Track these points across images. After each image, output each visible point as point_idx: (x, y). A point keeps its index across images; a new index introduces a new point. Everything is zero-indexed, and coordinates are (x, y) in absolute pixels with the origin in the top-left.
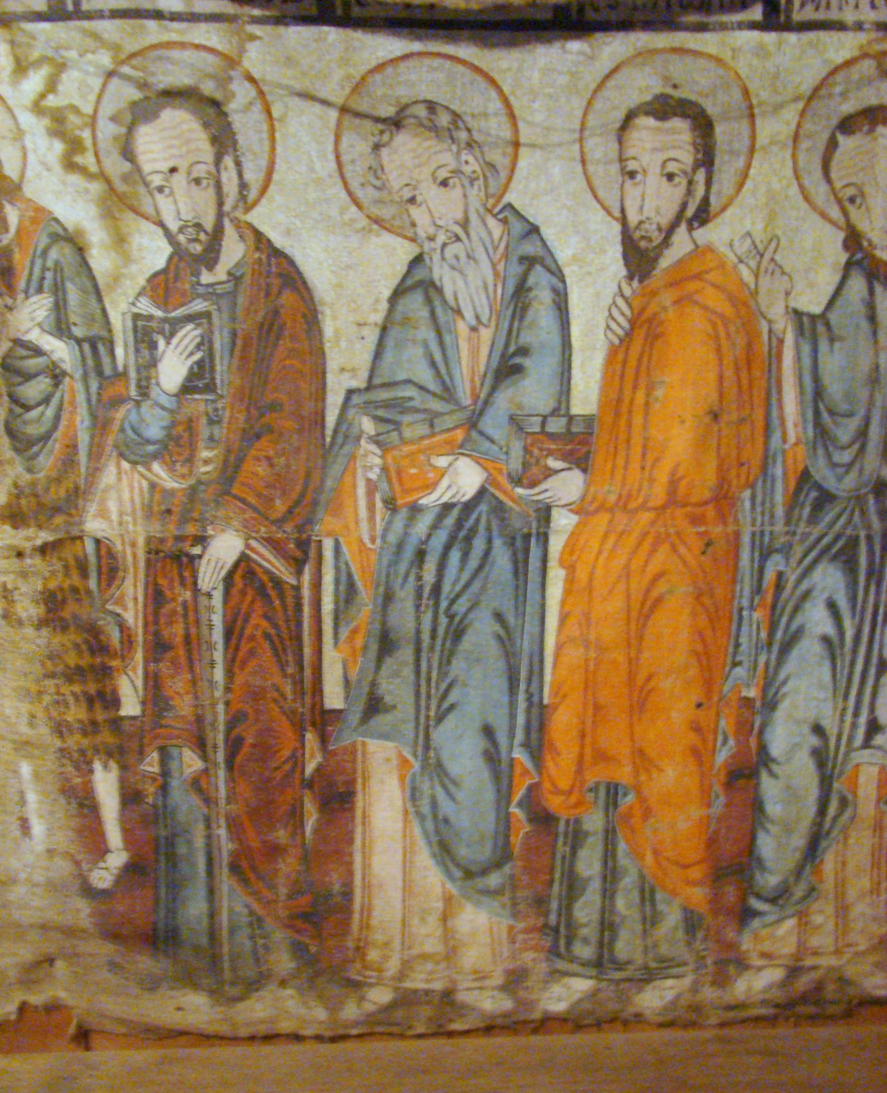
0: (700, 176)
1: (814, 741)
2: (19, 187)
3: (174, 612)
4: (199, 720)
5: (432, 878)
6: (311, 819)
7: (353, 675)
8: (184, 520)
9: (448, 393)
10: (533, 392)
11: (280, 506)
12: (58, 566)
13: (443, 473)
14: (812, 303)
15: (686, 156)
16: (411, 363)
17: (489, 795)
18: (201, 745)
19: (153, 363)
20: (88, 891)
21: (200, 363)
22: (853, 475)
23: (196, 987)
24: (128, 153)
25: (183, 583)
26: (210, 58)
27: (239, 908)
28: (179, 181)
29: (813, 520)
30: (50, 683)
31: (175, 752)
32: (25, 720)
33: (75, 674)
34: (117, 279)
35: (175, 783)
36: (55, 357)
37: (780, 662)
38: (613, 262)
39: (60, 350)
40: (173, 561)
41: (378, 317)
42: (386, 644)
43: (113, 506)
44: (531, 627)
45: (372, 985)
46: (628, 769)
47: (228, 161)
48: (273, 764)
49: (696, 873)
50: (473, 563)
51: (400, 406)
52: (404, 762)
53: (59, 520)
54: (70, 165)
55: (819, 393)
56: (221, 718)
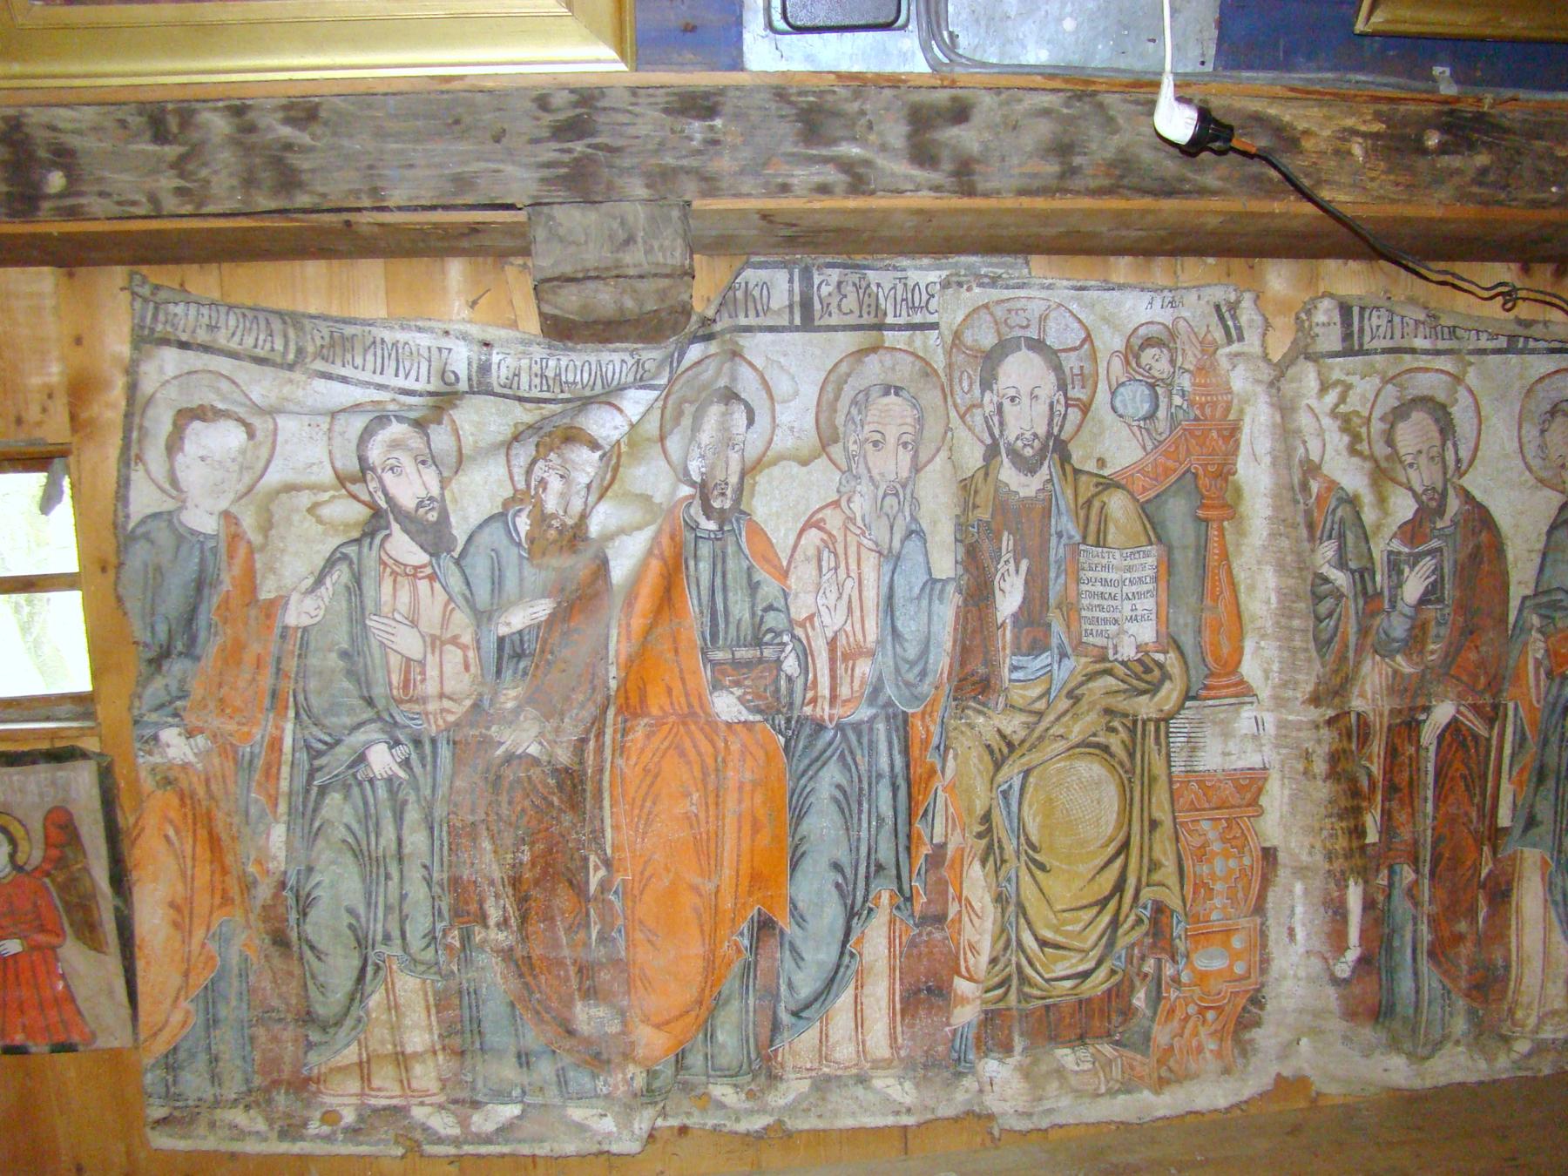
2: (1319, 467)
3: (1402, 764)
4: (1416, 842)
7: (1519, 804)
8: (1414, 697)
12: (1336, 734)
18: (1415, 861)
19: (1400, 585)
20: (1335, 981)
21: (1434, 584)
23: (1399, 1050)
24: (1390, 442)
25: (1410, 741)
26: (1444, 377)
27: (1435, 984)
28: (1423, 460)
31: (1397, 868)
34: (1378, 527)
35: (1396, 892)
36: (1337, 583)
39: (1340, 578)
40: (1408, 725)
41: (1540, 546)
43: (1368, 688)
45: (1517, 1039)
47: (1449, 444)
48: (1460, 872)
52: (1545, 862)
53: (1337, 700)
54: (1353, 451)
56: (1429, 840)
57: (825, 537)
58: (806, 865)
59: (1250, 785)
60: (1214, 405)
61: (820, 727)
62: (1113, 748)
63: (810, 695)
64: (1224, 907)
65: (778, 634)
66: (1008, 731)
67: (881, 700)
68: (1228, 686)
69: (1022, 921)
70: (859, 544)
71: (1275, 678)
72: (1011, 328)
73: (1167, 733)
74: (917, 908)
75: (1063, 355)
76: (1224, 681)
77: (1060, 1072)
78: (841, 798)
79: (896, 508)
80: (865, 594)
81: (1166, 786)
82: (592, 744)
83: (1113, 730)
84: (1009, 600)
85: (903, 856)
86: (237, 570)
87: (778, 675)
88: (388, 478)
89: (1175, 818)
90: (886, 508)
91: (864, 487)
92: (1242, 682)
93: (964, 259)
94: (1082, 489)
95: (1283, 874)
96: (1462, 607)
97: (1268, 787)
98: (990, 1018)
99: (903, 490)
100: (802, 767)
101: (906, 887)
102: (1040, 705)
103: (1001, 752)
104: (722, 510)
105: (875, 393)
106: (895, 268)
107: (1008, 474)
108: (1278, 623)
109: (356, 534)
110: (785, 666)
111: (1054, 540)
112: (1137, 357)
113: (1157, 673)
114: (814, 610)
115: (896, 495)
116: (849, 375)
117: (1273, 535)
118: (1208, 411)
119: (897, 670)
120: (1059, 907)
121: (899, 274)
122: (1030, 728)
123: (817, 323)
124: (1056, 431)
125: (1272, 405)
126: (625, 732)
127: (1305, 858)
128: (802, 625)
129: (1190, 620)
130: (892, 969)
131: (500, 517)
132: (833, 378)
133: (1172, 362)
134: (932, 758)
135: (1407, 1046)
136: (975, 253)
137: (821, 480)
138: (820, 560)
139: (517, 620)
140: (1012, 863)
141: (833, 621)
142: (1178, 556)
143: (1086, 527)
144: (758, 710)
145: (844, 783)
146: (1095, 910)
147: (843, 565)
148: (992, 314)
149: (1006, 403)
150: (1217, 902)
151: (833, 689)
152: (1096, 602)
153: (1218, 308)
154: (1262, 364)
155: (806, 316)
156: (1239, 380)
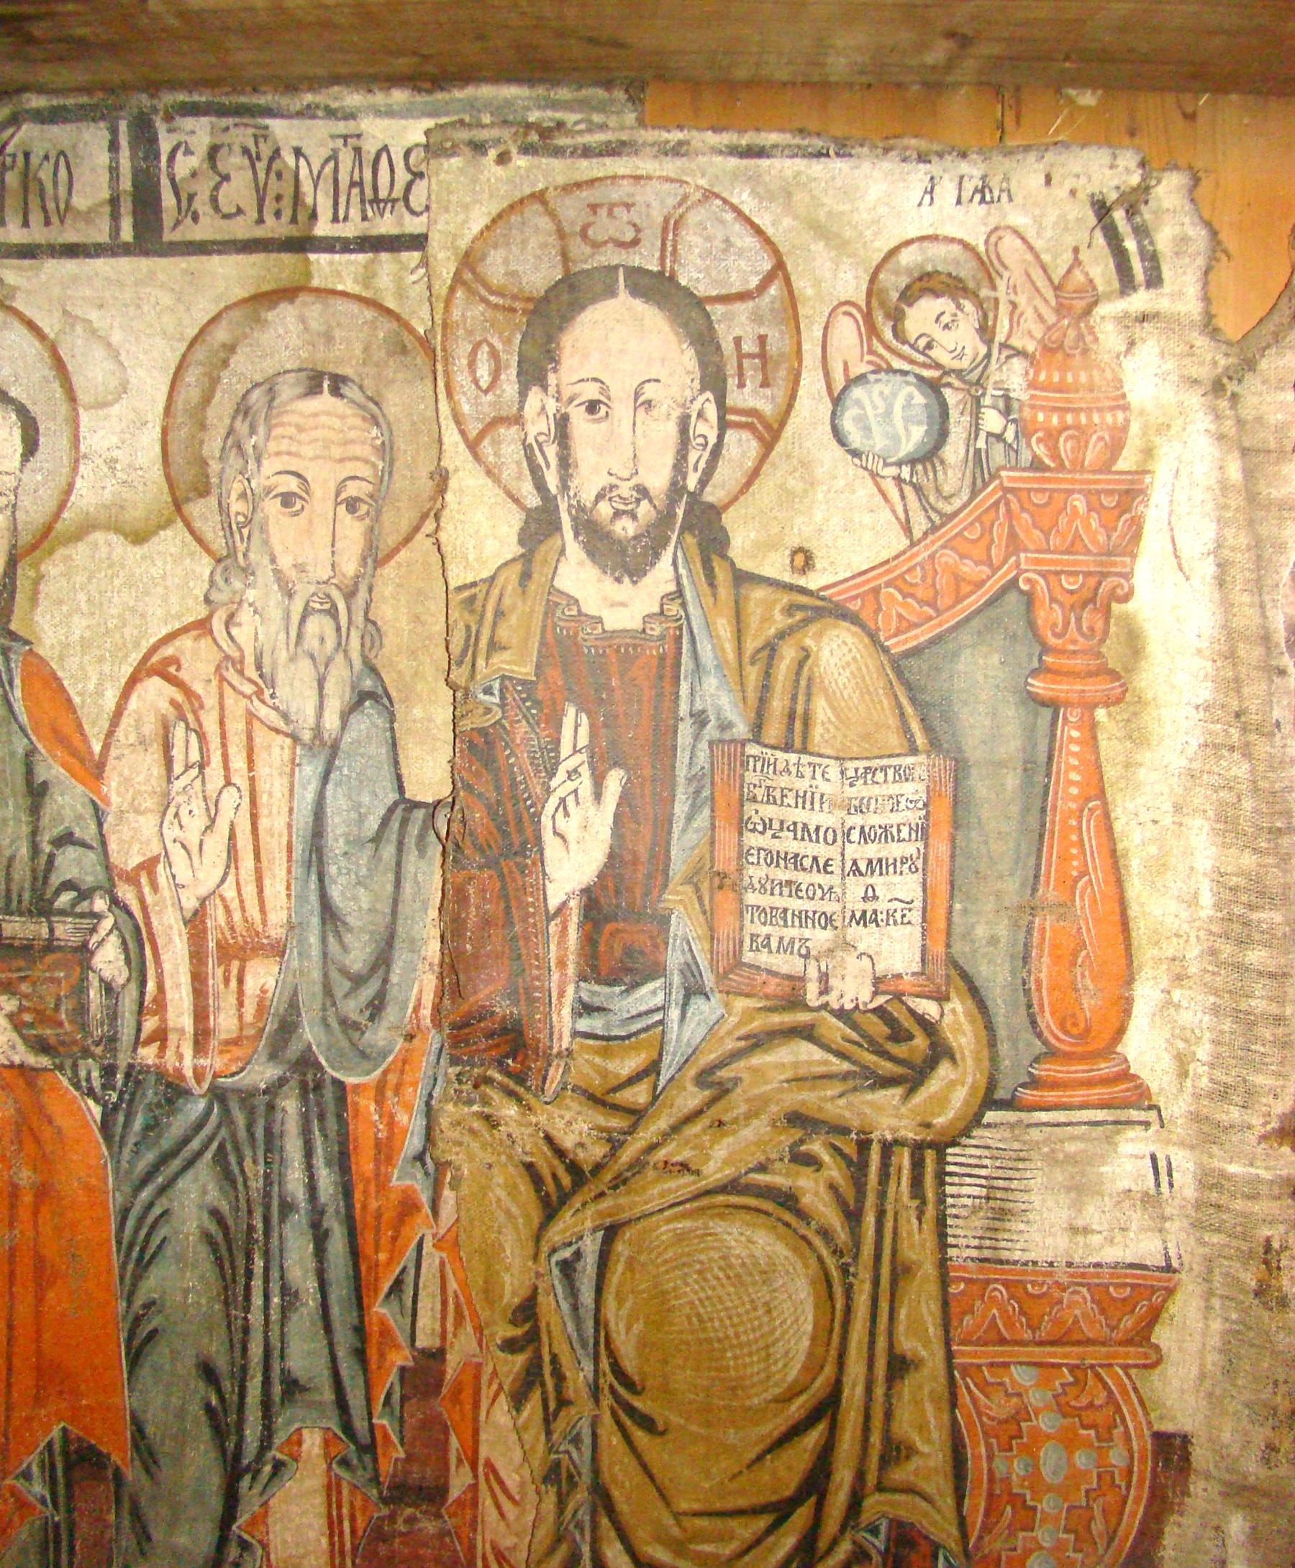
32: (1255, 1454)
57: (180, 698)
58: (159, 1354)
59: (1137, 1302)
60: (1081, 434)
61: (174, 1091)
62: (806, 1200)
63: (150, 1024)
64: (1059, 1547)
66: (568, 1142)
68: (1089, 1083)
69: (605, 1522)
70: (251, 717)
72: (596, 245)
73: (941, 1176)
74: (386, 1468)
75: (717, 311)
76: (1078, 1070)
78: (220, 1238)
79: (330, 643)
80: (264, 823)
81: (933, 1288)
83: (811, 1161)
84: (574, 853)
85: (348, 1368)
87: (84, 979)
89: (949, 1355)
90: (311, 642)
91: (262, 592)
92: (1125, 1075)
93: (486, 91)
94: (753, 620)
95: (1201, 1492)
97: (1174, 1307)
99: (349, 601)
100: (142, 1165)
101: (360, 1424)
102: (639, 1095)
103: (558, 1183)
105: (286, 390)
106: (331, 113)
107: (578, 576)
108: (1213, 952)
110: (99, 961)
111: (685, 732)
112: (897, 318)
113: (920, 1042)
114: (156, 849)
115: (333, 613)
116: (231, 348)
117: (1212, 747)
118: (1065, 447)
119: (328, 991)
120: (684, 1506)
121: (341, 127)
123: (168, 236)
124: (692, 482)
125: (1221, 437)
128: (132, 878)
129: (1002, 930)
132: (200, 354)
133: (986, 332)
136: (518, 81)
137: (169, 578)
138: (167, 747)
140: (581, 1412)
141: (197, 874)
142: (979, 785)
143: (763, 701)
144: (42, 1047)
145: (225, 1207)
146: (762, 1522)
147: (216, 758)
148: (552, 214)
149: (578, 417)
150: (1043, 1535)
151: (201, 1015)
152: (782, 875)
153: (1102, 209)
154: (1201, 342)
155: (146, 224)
156: (1150, 377)
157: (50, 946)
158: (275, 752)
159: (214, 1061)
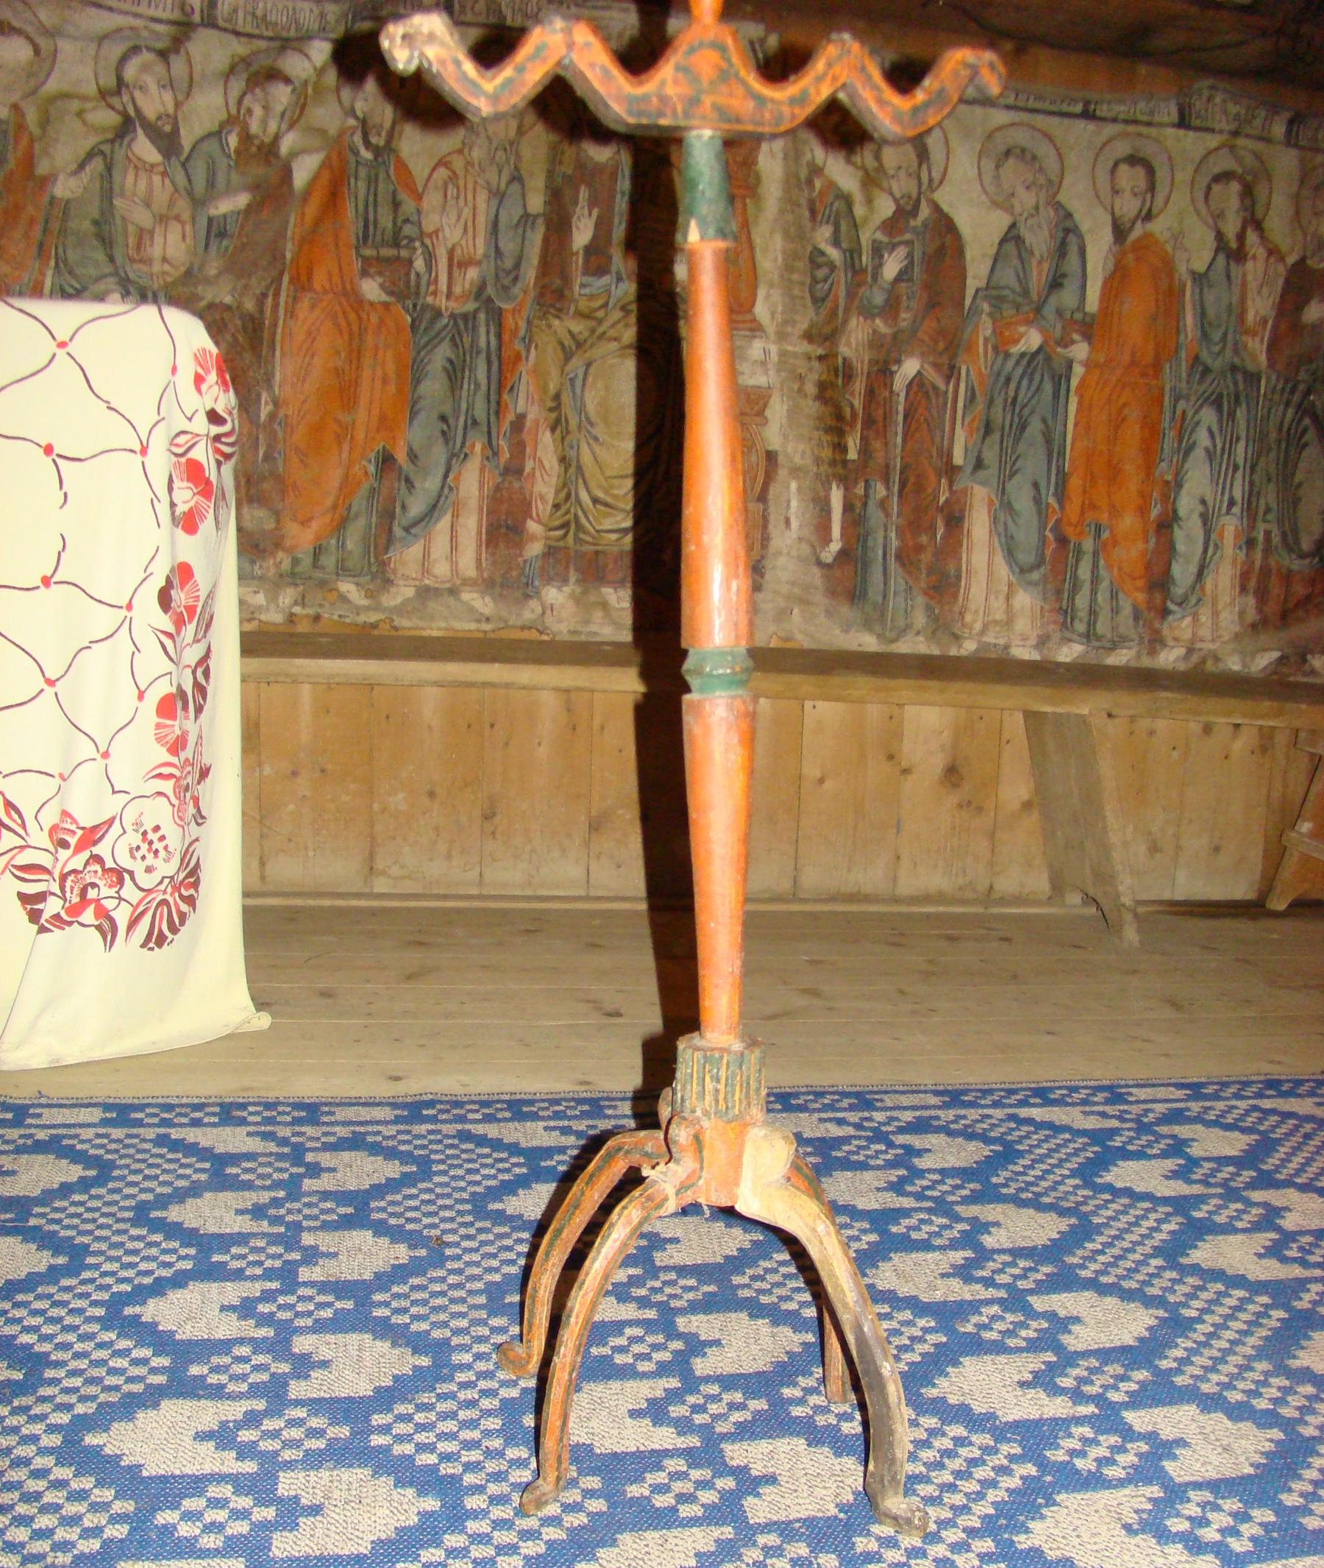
0: (1149, 196)
1: (1200, 508)
5: (1003, 570)
6: (940, 533)
9: (1026, 293)
10: (1067, 297)
11: (941, 345)
13: (1021, 336)
14: (1200, 266)
15: (1142, 184)
16: (1008, 277)
17: (1035, 522)
18: (887, 481)
19: (881, 265)
20: (819, 563)
22: (1220, 360)
28: (902, 174)
29: (1200, 383)
30: (816, 434)
33: (828, 430)
34: (866, 220)
37: (1184, 461)
38: (1107, 235)
39: (834, 254)
40: (883, 371)
41: (994, 251)
42: (988, 429)
43: (853, 340)
44: (1059, 428)
46: (1106, 515)
47: (924, 167)
49: (1140, 583)
50: (1033, 388)
51: (1001, 299)
52: (991, 503)
55: (1203, 314)
61: (438, 314)
63: (432, 288)
65: (411, 240)
67: (484, 296)
71: (779, 318)
77: (604, 605)
82: (270, 301)
85: (493, 418)
86: (19, 154)
88: (137, 94)
91: (482, 141)
92: (754, 320)
95: (782, 473)
96: (927, 286)
97: (772, 401)
98: (550, 552)
102: (600, 314)
104: (377, 147)
109: (110, 136)
117: (782, 211)
120: (609, 473)
122: (593, 331)
126: (295, 299)
127: (798, 460)
128: (430, 236)
130: (481, 509)
131: (217, 135)
134: (519, 346)
135: (878, 628)
139: (224, 207)
141: (452, 235)
144: (391, 293)
157: (398, 258)
158: (482, 196)
159: (452, 304)
